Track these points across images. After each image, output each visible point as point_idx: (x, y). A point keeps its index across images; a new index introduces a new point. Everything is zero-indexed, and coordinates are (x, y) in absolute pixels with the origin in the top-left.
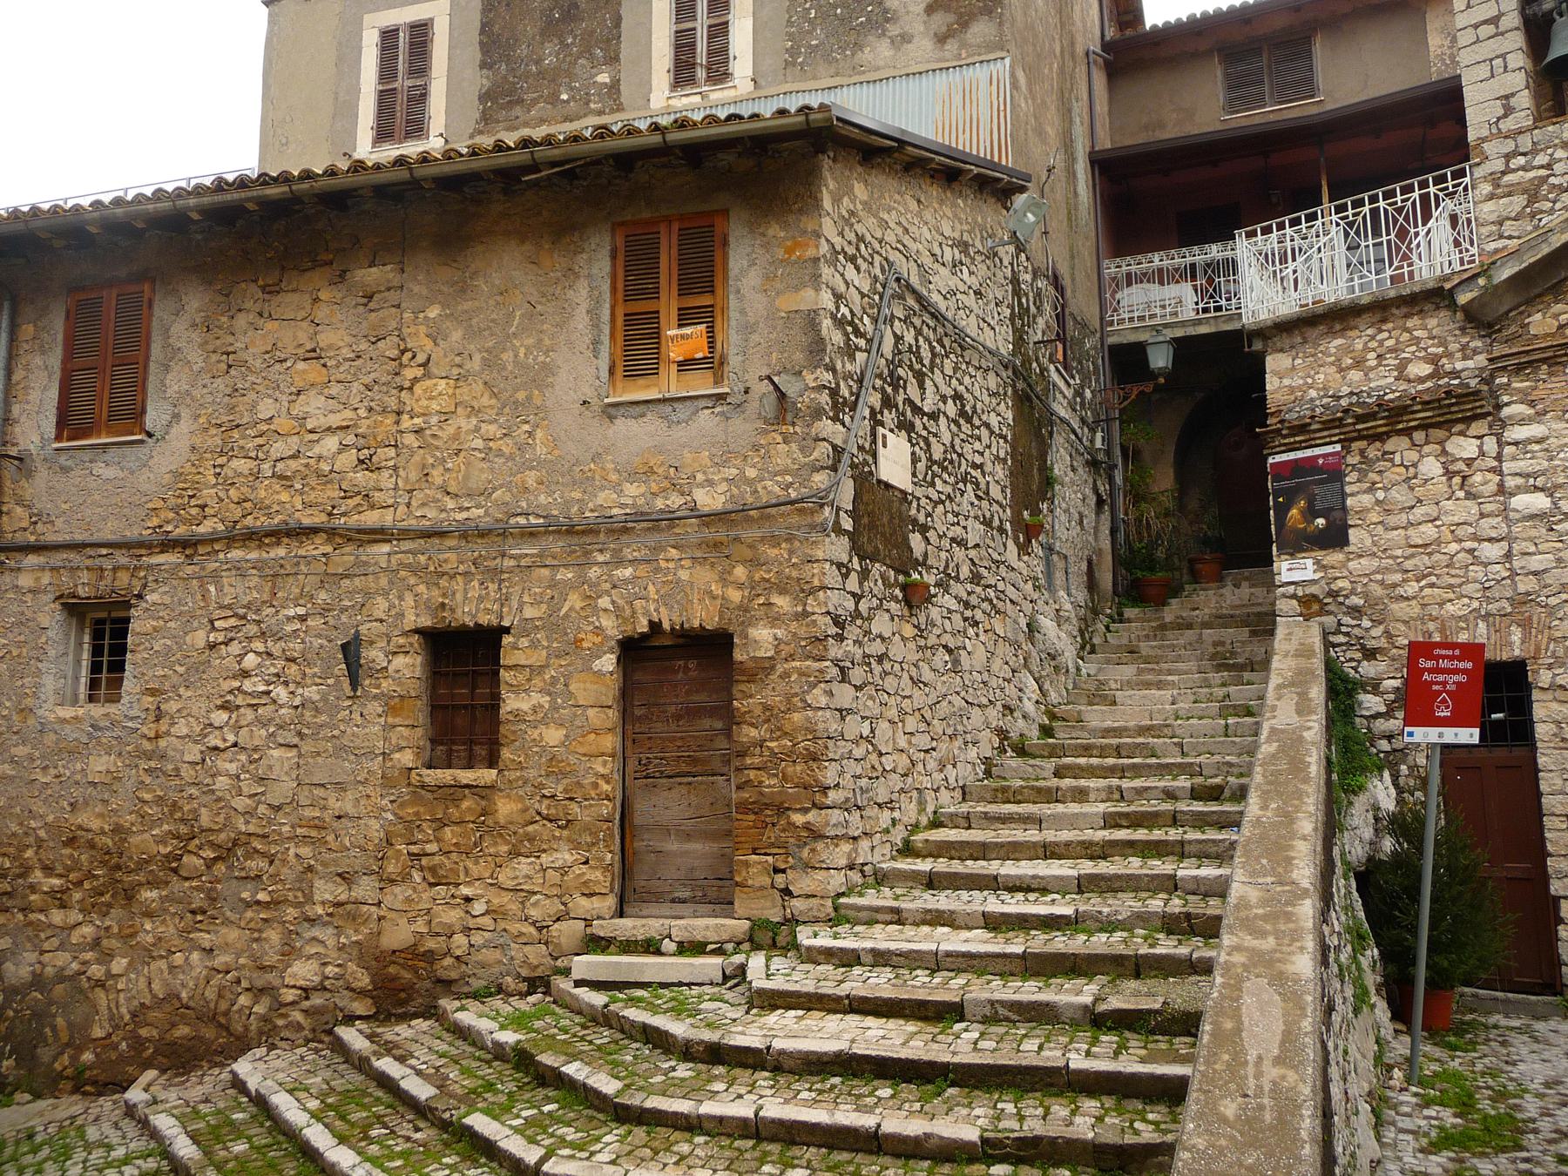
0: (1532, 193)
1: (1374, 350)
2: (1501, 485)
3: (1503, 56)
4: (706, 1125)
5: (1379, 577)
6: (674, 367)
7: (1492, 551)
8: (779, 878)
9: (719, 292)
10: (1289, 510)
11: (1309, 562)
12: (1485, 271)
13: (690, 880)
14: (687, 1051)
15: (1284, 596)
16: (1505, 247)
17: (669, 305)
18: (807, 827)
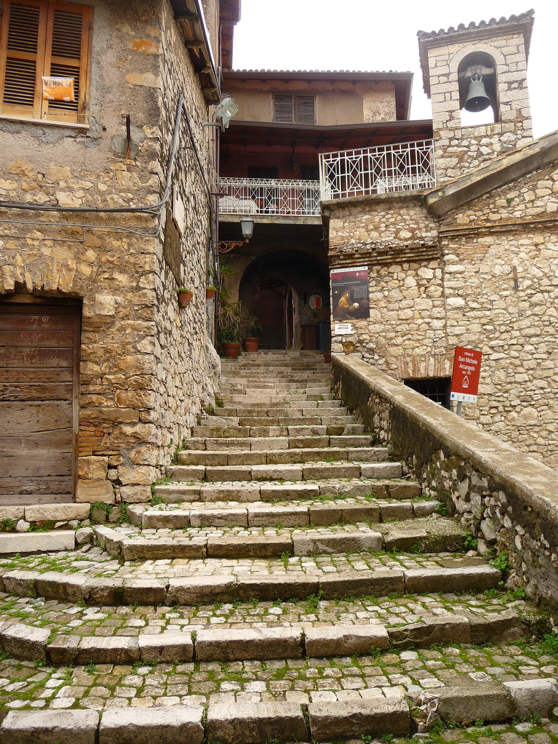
0: (461, 157)
1: (384, 223)
2: (443, 293)
3: (450, 92)
4: (146, 656)
5: (384, 334)
6: (46, 103)
7: (437, 324)
8: (113, 473)
9: (84, 59)
10: (340, 298)
11: (349, 325)
12: (441, 189)
13: (37, 477)
14: (90, 598)
15: (336, 342)
16: (448, 181)
17: (44, 60)
18: (135, 436)
